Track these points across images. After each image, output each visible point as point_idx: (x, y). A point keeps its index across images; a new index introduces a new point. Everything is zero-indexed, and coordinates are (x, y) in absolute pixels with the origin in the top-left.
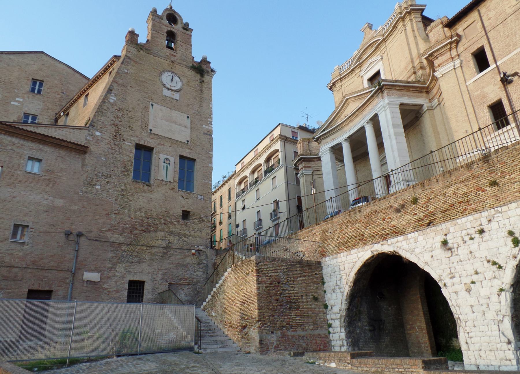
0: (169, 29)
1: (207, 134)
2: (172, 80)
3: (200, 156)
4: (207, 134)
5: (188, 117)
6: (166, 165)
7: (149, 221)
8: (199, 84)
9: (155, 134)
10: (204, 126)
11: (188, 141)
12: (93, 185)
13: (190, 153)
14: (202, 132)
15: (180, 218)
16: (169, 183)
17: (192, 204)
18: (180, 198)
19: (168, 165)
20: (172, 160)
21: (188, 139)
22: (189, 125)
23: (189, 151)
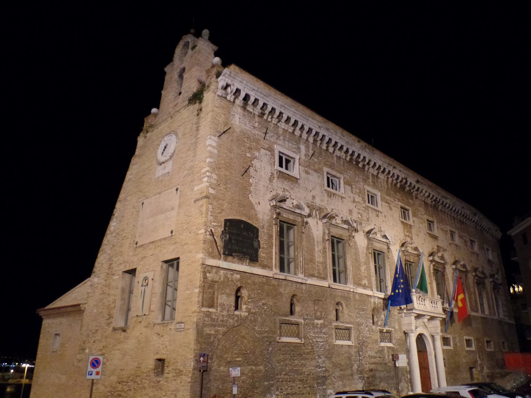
0: (178, 70)
1: (198, 200)
2: (165, 147)
3: (185, 247)
4: (198, 200)
5: (177, 190)
6: (143, 288)
7: (120, 387)
8: (195, 120)
9: (141, 246)
10: (196, 188)
11: (172, 232)
12: (83, 349)
13: (174, 250)
14: (193, 200)
15: (152, 375)
16: (145, 317)
17: (167, 343)
18: (155, 338)
19: (146, 288)
20: (150, 276)
21: (173, 228)
22: (177, 203)
23: (173, 247)
